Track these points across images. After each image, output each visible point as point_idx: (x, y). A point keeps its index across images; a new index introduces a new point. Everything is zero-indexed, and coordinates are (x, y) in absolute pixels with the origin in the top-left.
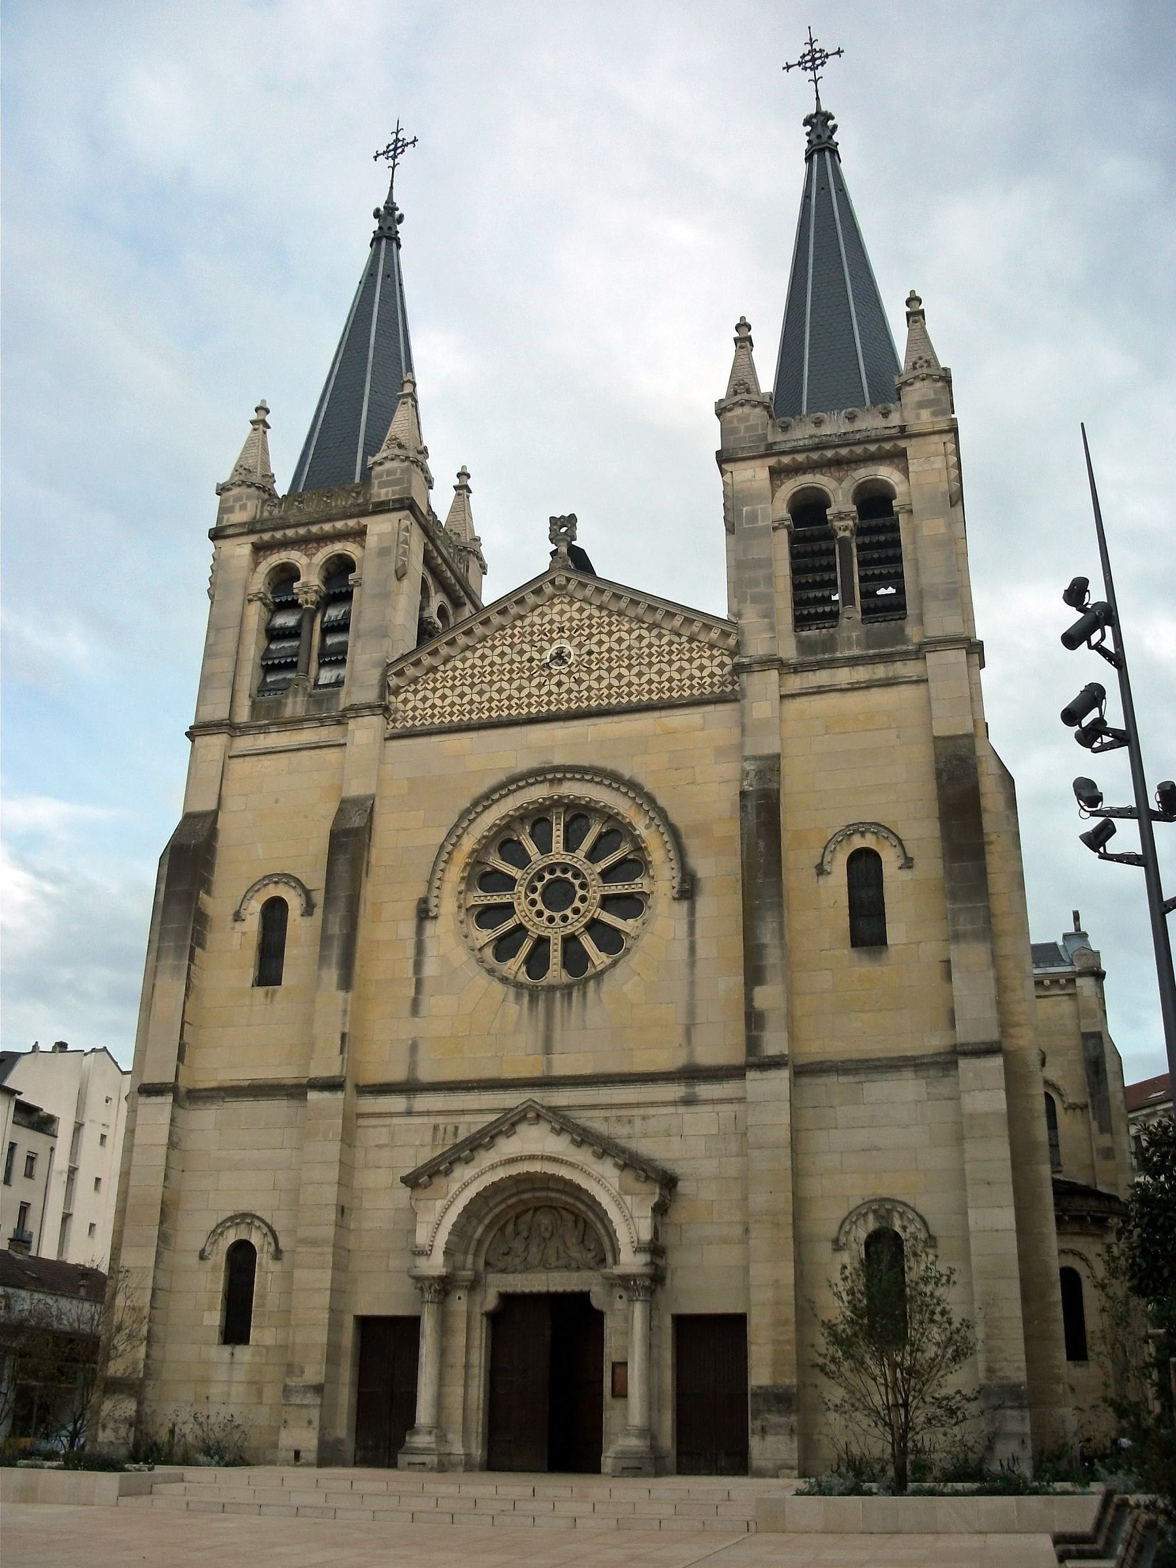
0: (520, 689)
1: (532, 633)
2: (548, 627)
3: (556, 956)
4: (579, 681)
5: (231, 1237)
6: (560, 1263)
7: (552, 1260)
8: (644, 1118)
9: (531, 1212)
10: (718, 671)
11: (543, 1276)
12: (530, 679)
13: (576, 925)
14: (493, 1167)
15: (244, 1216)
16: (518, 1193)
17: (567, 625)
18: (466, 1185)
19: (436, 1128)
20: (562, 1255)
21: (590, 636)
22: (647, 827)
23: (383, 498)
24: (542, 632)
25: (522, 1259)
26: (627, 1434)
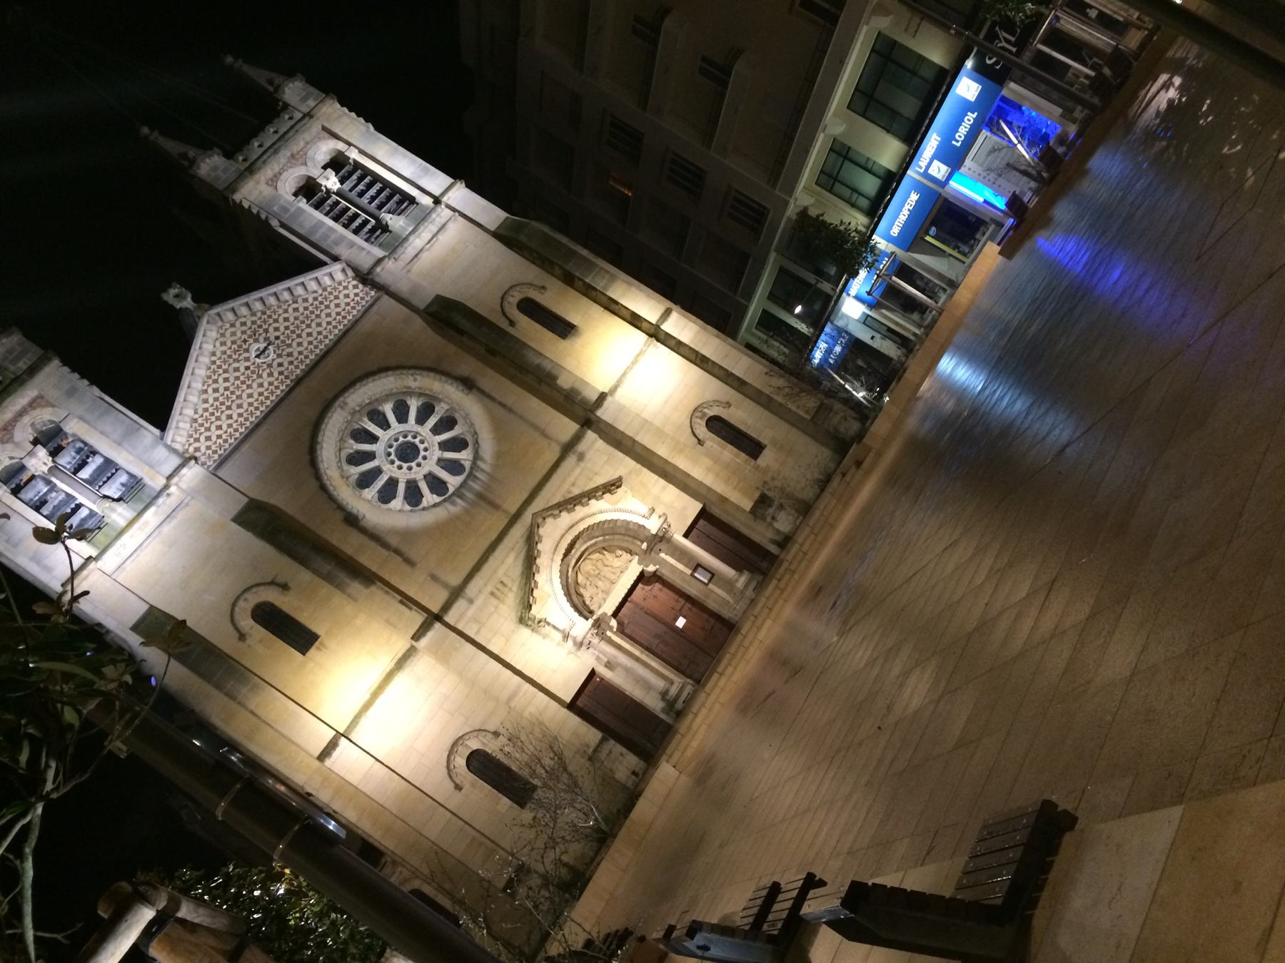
0: (261, 385)
1: (230, 357)
2: (235, 346)
3: (443, 475)
4: (290, 355)
5: (460, 761)
7: (613, 577)
8: (573, 485)
10: (356, 291)
12: (260, 376)
13: (437, 453)
15: (455, 744)
17: (245, 336)
18: (551, 580)
19: (492, 594)
21: (266, 331)
22: (415, 380)
23: (25, 367)
24: (235, 352)
26: (737, 581)
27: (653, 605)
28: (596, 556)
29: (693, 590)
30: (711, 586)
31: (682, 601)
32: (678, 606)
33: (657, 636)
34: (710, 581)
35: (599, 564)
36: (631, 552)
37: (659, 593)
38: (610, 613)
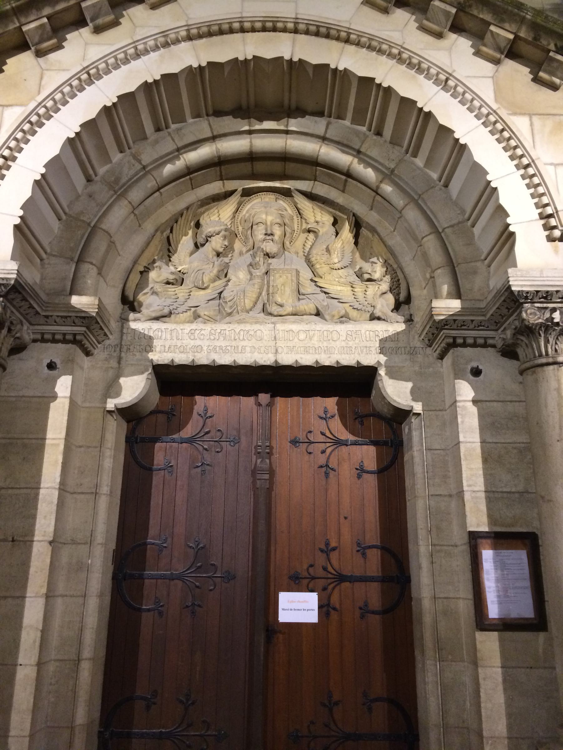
6: (308, 306)
7: (286, 297)
9: (233, 201)
14: (166, 42)
16: (214, 138)
20: (309, 288)
25: (210, 293)
27: (295, 472)
28: (319, 217)
29: (433, 581)
30: (489, 644)
31: (373, 564)
32: (352, 564)
33: (200, 555)
34: (506, 626)
35: (301, 241)
36: (402, 303)
37: (347, 472)
38: (160, 355)
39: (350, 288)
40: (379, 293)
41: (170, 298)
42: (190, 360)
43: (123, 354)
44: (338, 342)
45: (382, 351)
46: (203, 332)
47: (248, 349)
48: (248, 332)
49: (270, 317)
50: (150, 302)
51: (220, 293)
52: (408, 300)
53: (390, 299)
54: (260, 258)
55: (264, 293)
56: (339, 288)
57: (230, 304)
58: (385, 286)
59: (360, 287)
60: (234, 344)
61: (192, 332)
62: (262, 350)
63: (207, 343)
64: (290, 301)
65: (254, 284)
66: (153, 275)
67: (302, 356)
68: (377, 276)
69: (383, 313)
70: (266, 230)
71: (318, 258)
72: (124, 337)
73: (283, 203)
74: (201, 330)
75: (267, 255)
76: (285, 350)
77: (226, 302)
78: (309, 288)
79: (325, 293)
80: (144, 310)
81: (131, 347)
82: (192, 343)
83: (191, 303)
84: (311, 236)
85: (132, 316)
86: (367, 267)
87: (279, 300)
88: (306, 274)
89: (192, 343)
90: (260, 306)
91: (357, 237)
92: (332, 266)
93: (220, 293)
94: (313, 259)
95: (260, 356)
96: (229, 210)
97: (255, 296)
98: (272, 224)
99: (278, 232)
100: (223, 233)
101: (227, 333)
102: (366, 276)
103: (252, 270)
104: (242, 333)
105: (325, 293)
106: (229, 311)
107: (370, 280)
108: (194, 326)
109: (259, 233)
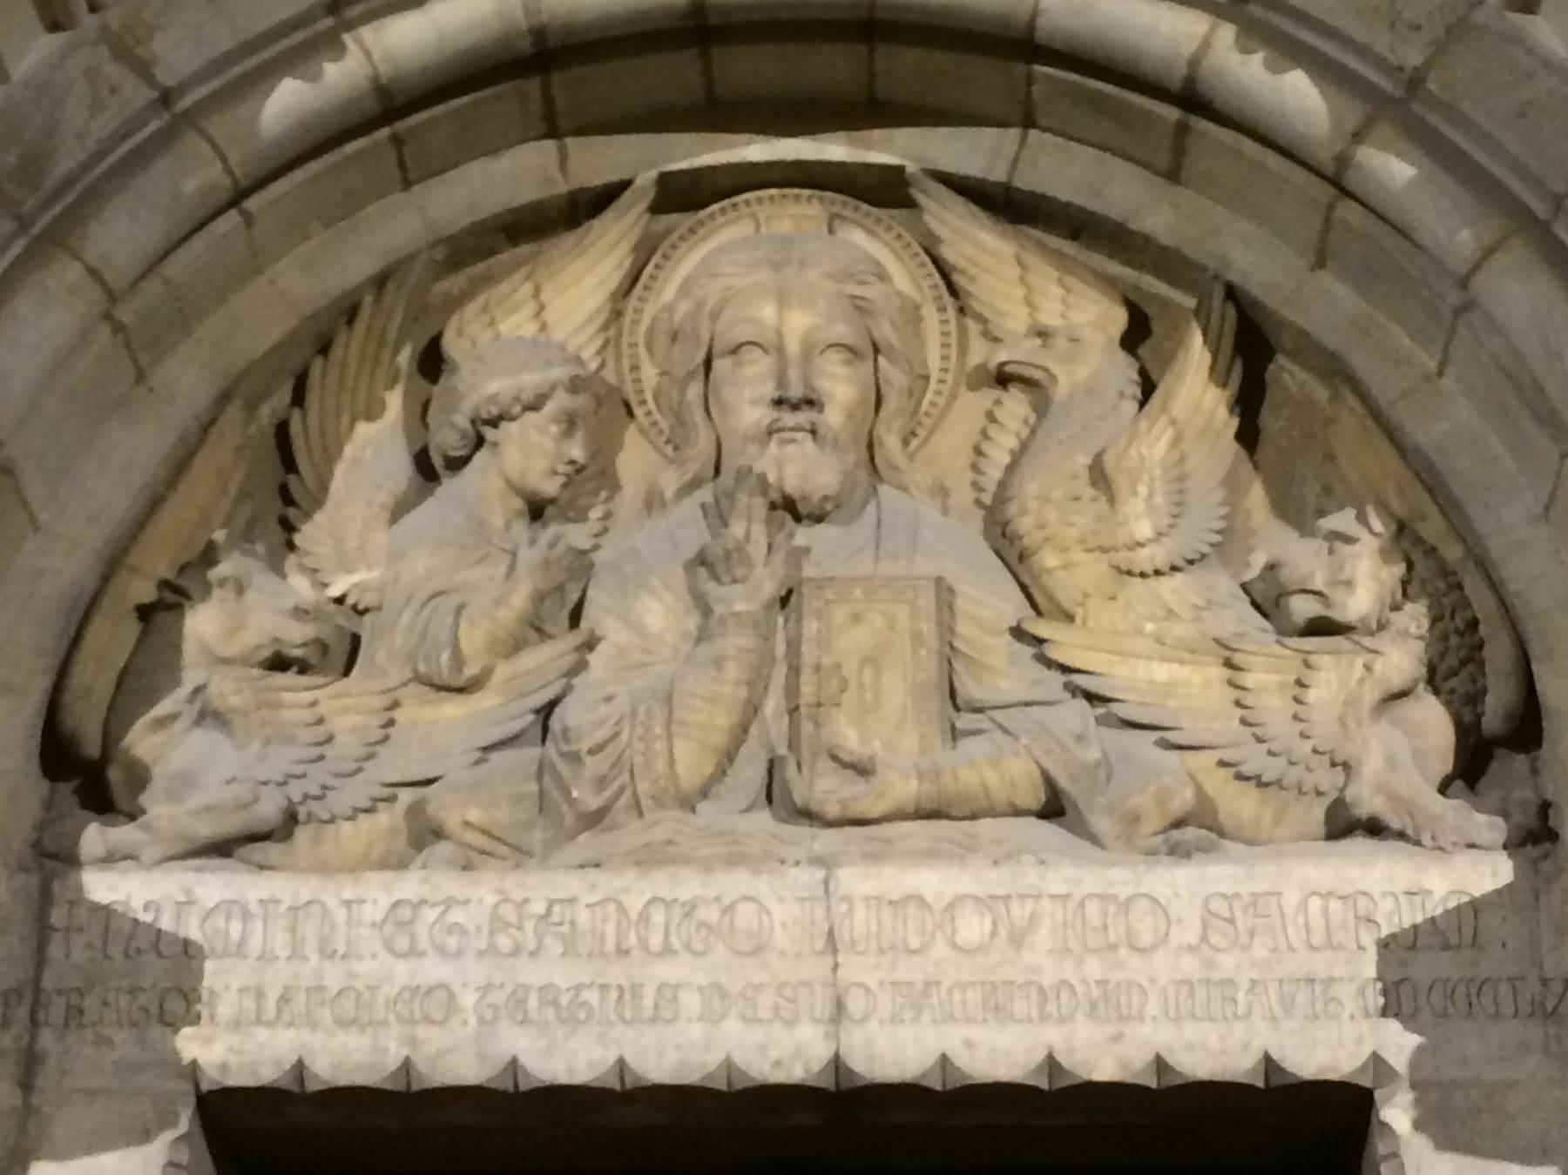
6: (999, 766)
11: (776, 896)
20: (1004, 674)
25: (495, 708)
28: (1057, 310)
35: (964, 434)
38: (231, 1044)
39: (1217, 672)
40: (1371, 695)
41: (289, 740)
42: (392, 1061)
43: (46, 1039)
44: (1160, 958)
45: (1396, 1001)
46: (456, 915)
47: (691, 1002)
48: (690, 908)
49: (803, 831)
50: (189, 762)
51: (546, 711)
52: (1527, 728)
53: (1433, 723)
54: (749, 526)
55: (773, 704)
56: (1162, 672)
57: (594, 766)
58: (1400, 659)
59: (1269, 667)
60: (617, 973)
61: (401, 917)
62: (766, 1000)
63: (478, 972)
64: (909, 742)
65: (718, 663)
66: (202, 623)
67: (976, 1033)
68: (1358, 604)
69: (1393, 798)
70: (781, 383)
71: (1052, 515)
72: (55, 950)
73: (867, 240)
74: (449, 903)
75: (789, 508)
76: (885, 1003)
77: (575, 758)
78: (1004, 674)
79: (1092, 698)
80: (156, 806)
81: (90, 1003)
82: (402, 971)
83: (396, 764)
84: (1015, 404)
85: (94, 836)
86: (1303, 559)
87: (850, 739)
88: (990, 601)
89: (402, 971)
90: (750, 772)
91: (1249, 405)
92: (1122, 558)
93: (546, 711)
94: (1024, 524)
95: (756, 1035)
96: (590, 281)
97: (725, 719)
98: (810, 350)
99: (841, 388)
100: (560, 401)
101: (583, 917)
102: (1303, 608)
103: (710, 587)
104: (658, 917)
105: (1092, 698)
106: (593, 802)
107: (1322, 627)
108: (409, 885)
109: (747, 399)
